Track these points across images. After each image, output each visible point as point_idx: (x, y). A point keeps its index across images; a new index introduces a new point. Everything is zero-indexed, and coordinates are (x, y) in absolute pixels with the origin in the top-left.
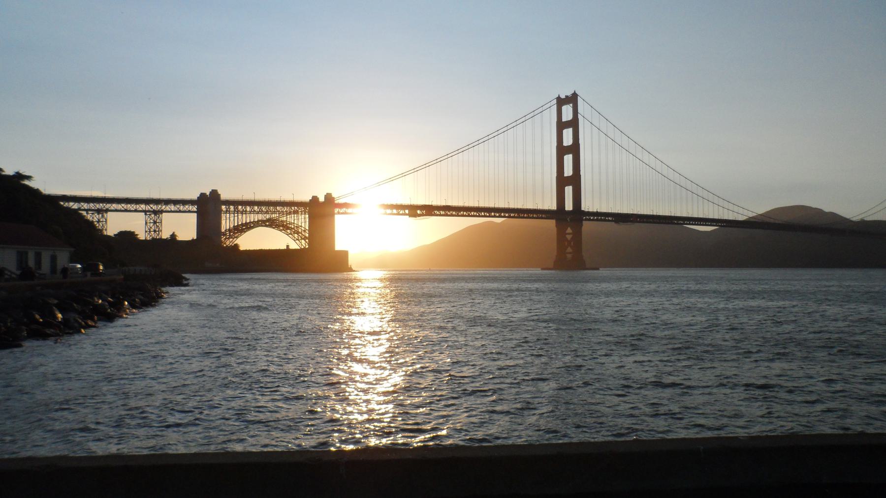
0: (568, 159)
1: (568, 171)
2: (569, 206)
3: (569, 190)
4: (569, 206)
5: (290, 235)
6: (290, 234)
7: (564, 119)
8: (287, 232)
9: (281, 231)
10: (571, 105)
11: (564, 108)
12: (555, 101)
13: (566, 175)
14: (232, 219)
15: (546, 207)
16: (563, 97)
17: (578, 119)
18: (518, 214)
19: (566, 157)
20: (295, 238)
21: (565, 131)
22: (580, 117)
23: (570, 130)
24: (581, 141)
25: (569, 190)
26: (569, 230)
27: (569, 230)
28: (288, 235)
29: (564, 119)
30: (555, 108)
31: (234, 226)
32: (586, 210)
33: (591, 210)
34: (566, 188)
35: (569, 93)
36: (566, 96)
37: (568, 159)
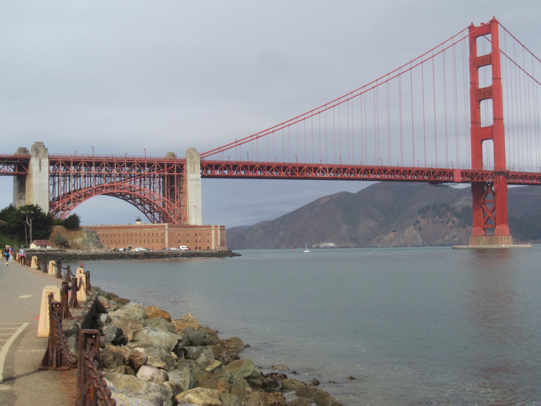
5: (140, 206)
6: (139, 204)
8: (135, 202)
9: (127, 200)
10: (489, 36)
11: (480, 40)
12: (467, 32)
13: (483, 125)
14: (62, 183)
16: (477, 24)
20: (145, 208)
21: (481, 70)
22: (500, 51)
23: (489, 68)
24: (503, 82)
25: (488, 146)
28: (136, 206)
29: (480, 53)
31: (64, 194)
32: (511, 170)
35: (487, 21)
36: (482, 23)
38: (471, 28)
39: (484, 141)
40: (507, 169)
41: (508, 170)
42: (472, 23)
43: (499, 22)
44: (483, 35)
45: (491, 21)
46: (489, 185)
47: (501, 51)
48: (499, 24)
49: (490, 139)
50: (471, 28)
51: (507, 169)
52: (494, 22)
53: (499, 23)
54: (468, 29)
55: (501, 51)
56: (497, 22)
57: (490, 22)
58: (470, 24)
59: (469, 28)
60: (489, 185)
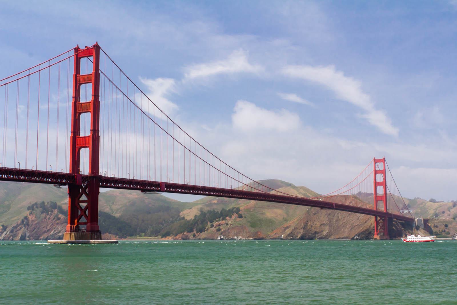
0: (86, 119)
1: (85, 131)
2: (85, 169)
3: (85, 154)
4: (85, 169)
7: (83, 73)
10: (92, 58)
11: (83, 61)
12: (73, 53)
13: (82, 135)
15: (59, 171)
16: (82, 47)
17: (99, 73)
18: (130, 185)
19: (82, 116)
22: (100, 72)
25: (85, 154)
26: (84, 198)
27: (84, 198)
30: (73, 60)
32: (103, 176)
33: (109, 175)
34: (82, 150)
35: (90, 45)
36: (86, 47)
37: (86, 119)
38: (77, 49)
39: (81, 148)
40: (99, 174)
41: (101, 175)
42: (78, 45)
43: (101, 47)
44: (87, 57)
45: (94, 46)
46: (84, 187)
47: (102, 72)
48: (100, 49)
49: (87, 147)
50: (77, 49)
51: (99, 174)
52: (97, 47)
53: (101, 48)
54: (74, 50)
55: (102, 72)
56: (100, 48)
57: (93, 47)
58: (76, 46)
59: (75, 49)
60: (84, 187)
